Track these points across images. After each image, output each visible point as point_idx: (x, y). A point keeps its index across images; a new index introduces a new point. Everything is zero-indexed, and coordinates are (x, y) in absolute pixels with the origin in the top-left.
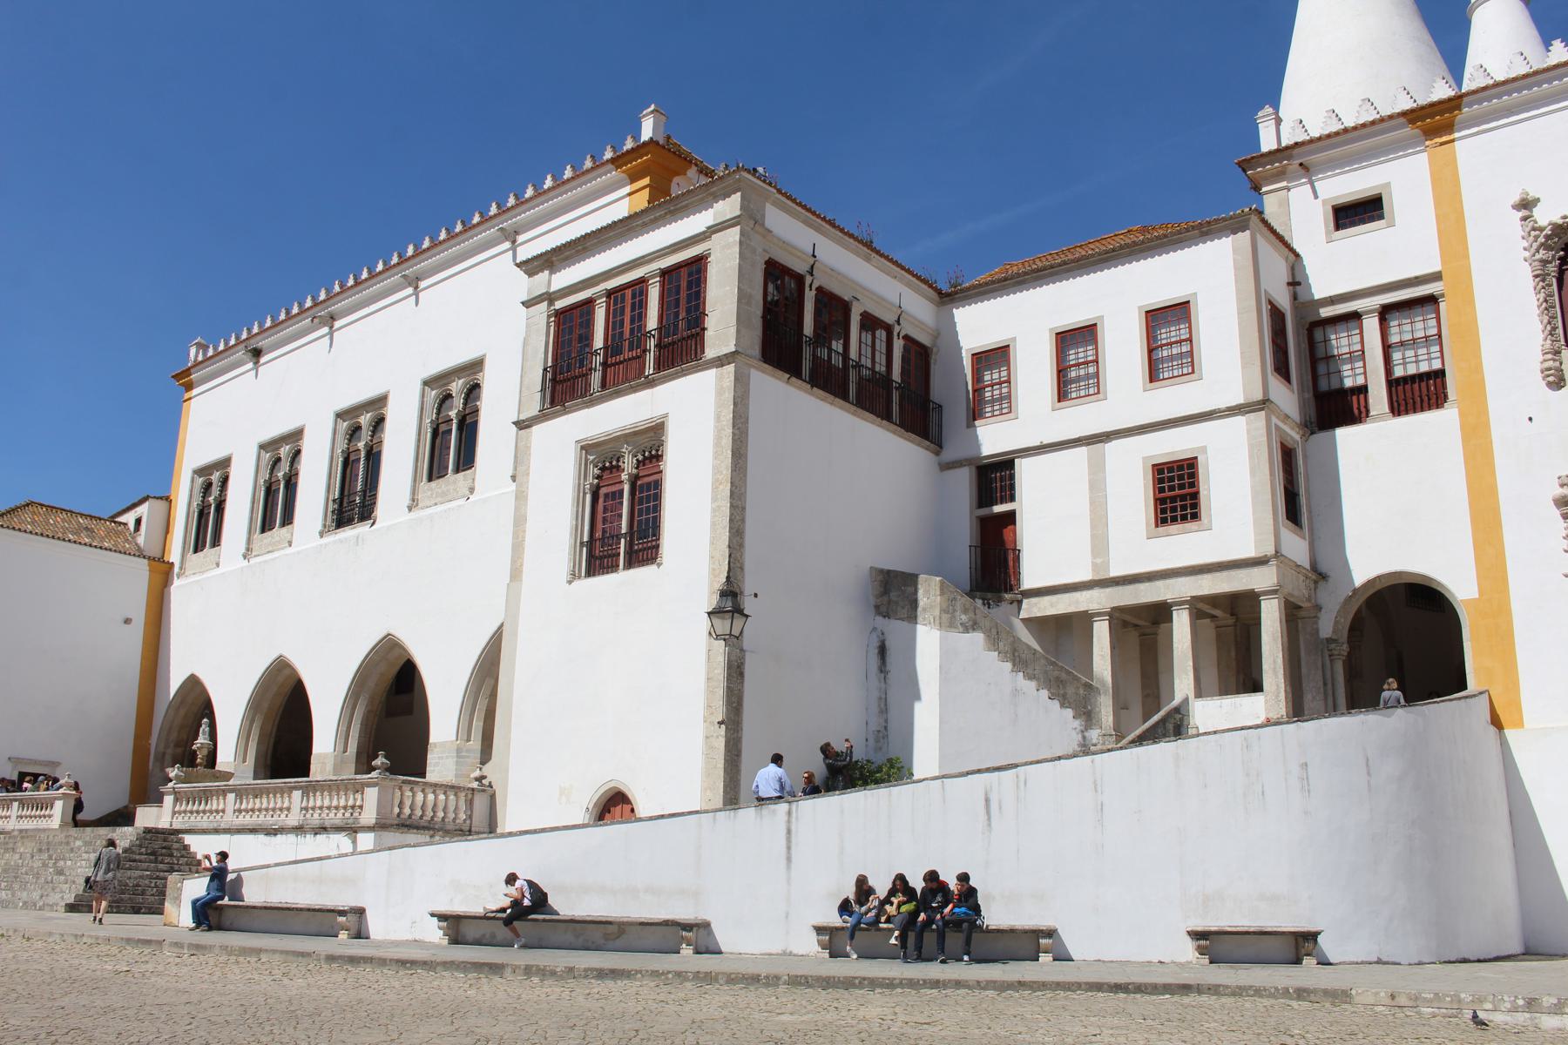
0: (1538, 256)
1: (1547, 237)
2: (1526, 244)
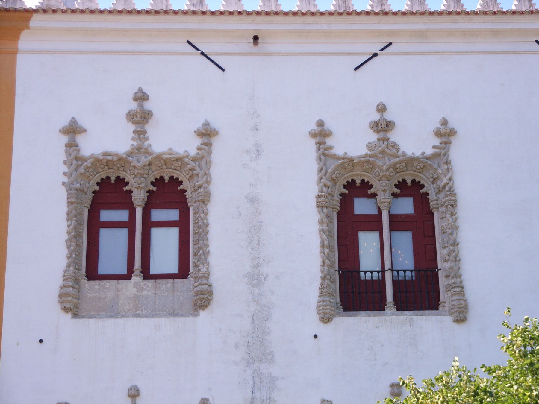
1: (87, 168)
2: (66, 170)
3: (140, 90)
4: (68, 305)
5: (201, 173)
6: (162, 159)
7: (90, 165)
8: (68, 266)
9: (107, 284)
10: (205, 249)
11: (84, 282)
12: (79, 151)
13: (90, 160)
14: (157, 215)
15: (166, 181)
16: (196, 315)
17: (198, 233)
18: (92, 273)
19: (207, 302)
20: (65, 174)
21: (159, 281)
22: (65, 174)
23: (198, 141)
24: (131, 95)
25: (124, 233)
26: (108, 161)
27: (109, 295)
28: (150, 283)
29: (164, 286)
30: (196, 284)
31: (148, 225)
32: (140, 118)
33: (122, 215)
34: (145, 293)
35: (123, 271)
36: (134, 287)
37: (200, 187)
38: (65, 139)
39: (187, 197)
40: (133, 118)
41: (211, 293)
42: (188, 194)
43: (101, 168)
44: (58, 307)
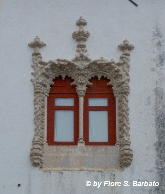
0: (40, 80)
1: (47, 69)
2: (33, 71)
3: (81, 18)
4: (36, 161)
5: (124, 73)
6: (97, 64)
7: (49, 67)
8: (36, 135)
9: (62, 148)
10: (127, 125)
11: (46, 145)
12: (41, 58)
13: (49, 65)
14: (93, 102)
15: (99, 79)
16: (123, 170)
17: (122, 114)
18: (51, 141)
19: (130, 161)
20: (32, 74)
21: (96, 147)
22: (32, 74)
23: (120, 54)
24: (75, 22)
25: (71, 114)
26: (61, 65)
27: (63, 155)
28: (90, 148)
29: (100, 150)
30: (121, 149)
31: (88, 109)
32: (80, 37)
33: (70, 102)
34: (87, 154)
35: (71, 139)
36: (80, 150)
37: (123, 83)
38: (32, 51)
39: (113, 90)
40: (77, 36)
41: (132, 156)
42: (114, 88)
43: (56, 70)
44: (30, 163)
